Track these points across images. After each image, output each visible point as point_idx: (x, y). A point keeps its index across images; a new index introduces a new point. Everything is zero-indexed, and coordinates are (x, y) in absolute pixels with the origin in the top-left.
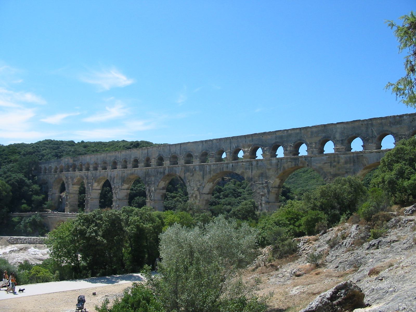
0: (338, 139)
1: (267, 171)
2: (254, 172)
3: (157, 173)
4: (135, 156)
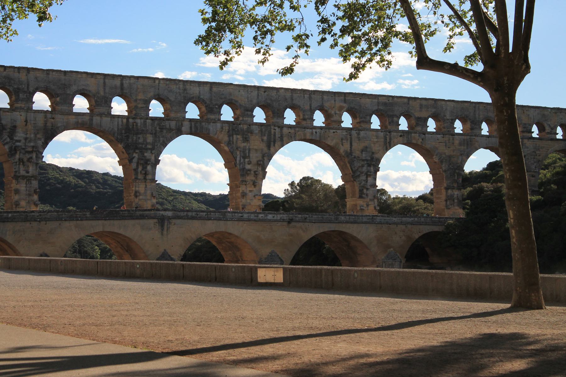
0: (448, 118)
1: (372, 145)
2: (355, 145)
3: (162, 129)
4: (84, 87)
